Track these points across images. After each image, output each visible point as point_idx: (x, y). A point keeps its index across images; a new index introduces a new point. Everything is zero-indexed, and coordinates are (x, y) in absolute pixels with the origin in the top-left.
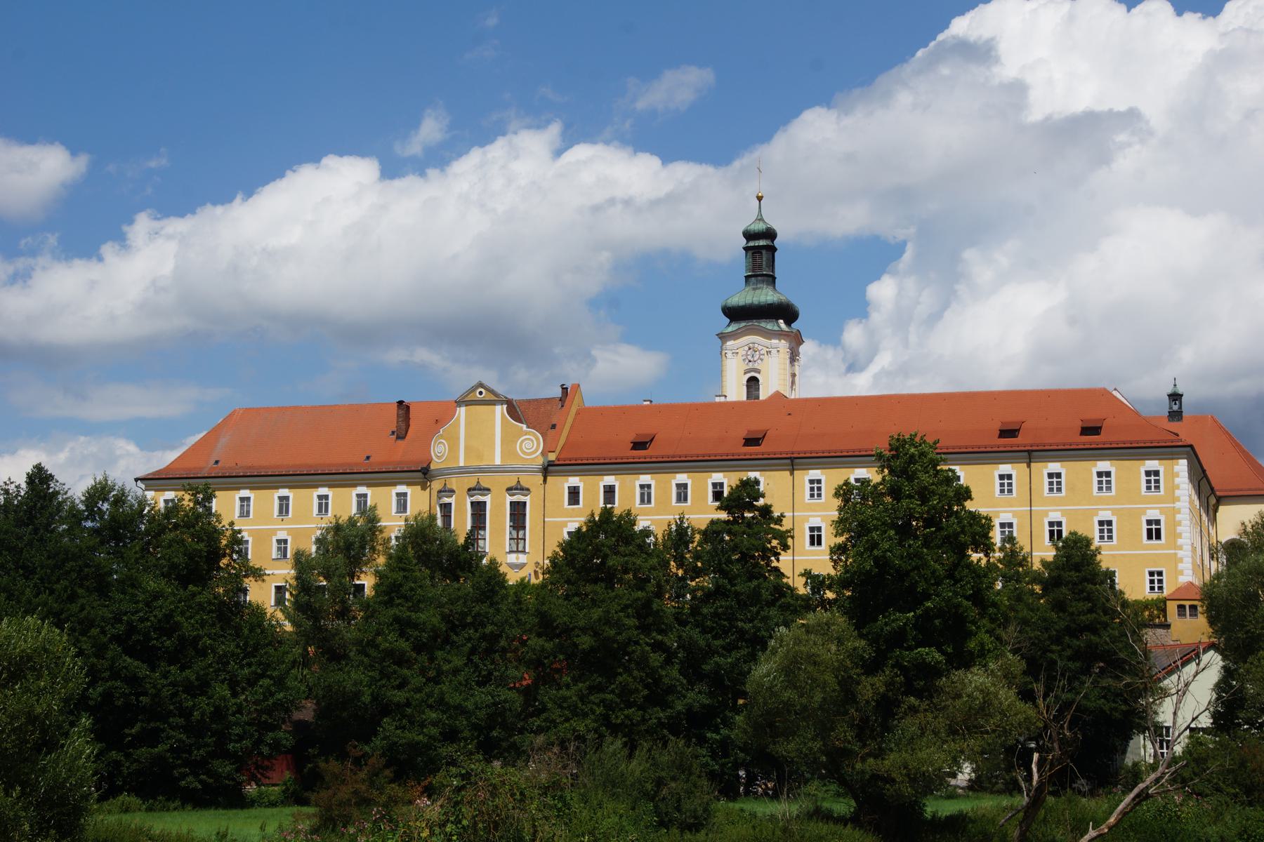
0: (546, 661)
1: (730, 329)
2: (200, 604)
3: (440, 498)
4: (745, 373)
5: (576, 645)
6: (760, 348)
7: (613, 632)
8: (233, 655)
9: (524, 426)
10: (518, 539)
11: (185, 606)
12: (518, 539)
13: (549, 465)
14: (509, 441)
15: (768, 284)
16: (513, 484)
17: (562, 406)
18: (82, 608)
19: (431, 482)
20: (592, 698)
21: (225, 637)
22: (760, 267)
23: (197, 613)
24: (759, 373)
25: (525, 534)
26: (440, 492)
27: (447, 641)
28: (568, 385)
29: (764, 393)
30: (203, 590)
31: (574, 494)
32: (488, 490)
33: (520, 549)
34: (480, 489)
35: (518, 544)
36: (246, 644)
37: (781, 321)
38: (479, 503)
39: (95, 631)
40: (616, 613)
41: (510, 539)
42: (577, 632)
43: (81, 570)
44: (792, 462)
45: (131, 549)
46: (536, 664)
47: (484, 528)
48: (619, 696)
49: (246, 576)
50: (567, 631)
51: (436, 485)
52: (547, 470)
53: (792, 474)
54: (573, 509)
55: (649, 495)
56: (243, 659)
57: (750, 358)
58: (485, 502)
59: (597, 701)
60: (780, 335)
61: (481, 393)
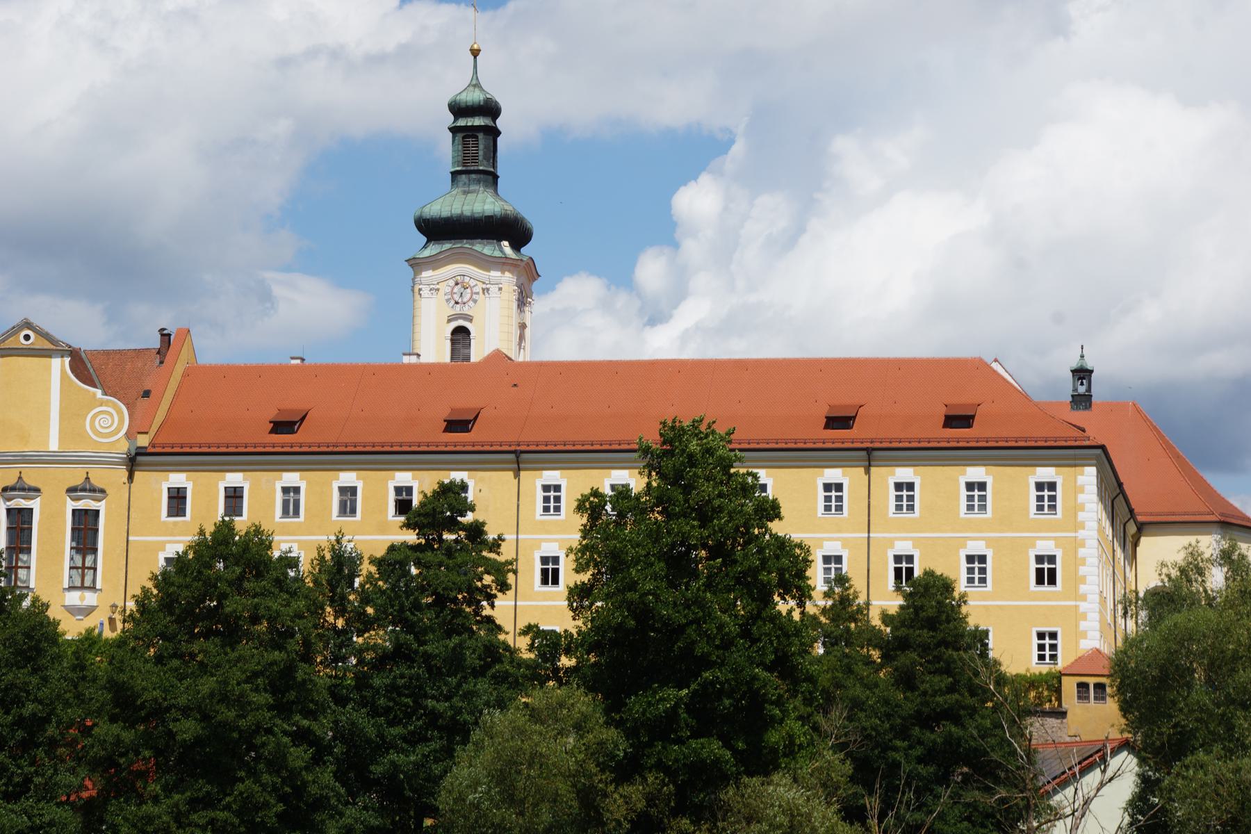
0: (122, 760)
1: (427, 253)
4: (449, 321)
5: (171, 735)
6: (472, 283)
7: (231, 714)
9: (99, 393)
10: (83, 567)
12: (83, 567)
13: (137, 454)
14: (72, 415)
15: (486, 186)
16: (78, 481)
17: (162, 362)
20: (194, 817)
22: (475, 158)
24: (471, 321)
25: (95, 561)
28: (171, 329)
29: (478, 351)
31: (177, 500)
32: (37, 490)
33: (88, 583)
34: (23, 489)
35: (84, 576)
37: (506, 243)
38: (20, 510)
40: (238, 684)
41: (71, 568)
42: (174, 713)
44: (518, 457)
46: (105, 764)
47: (28, 551)
48: (238, 814)
50: (158, 712)
52: (134, 461)
53: (517, 476)
54: (175, 523)
55: (297, 504)
57: (457, 297)
59: (202, 822)
60: (502, 264)
61: (27, 337)
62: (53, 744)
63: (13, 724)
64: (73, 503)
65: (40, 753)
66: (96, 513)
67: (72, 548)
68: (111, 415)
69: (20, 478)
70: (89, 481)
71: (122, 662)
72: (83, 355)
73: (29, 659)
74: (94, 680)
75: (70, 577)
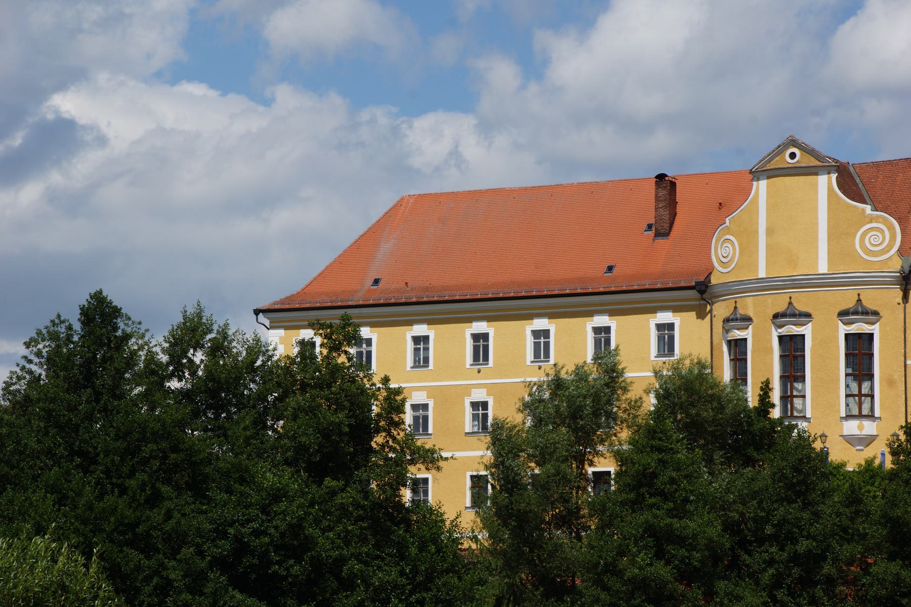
2: (342, 507)
3: (727, 331)
8: (396, 587)
9: (868, 208)
10: (860, 395)
11: (320, 509)
12: (860, 395)
16: (850, 304)
18: (168, 516)
19: (712, 304)
21: (383, 559)
23: (339, 521)
25: (872, 388)
26: (727, 320)
27: (735, 564)
30: (346, 485)
32: (808, 315)
33: (866, 411)
34: (794, 315)
36: (415, 570)
38: (792, 337)
39: (187, 552)
41: (847, 396)
43: (165, 457)
45: (238, 423)
47: (803, 379)
49: (413, 462)
51: (721, 310)
56: (412, 592)
58: (803, 336)
61: (793, 156)
62: (830, 582)
63: (789, 561)
64: (845, 327)
65: (819, 591)
66: (871, 336)
67: (847, 375)
68: (882, 231)
69: (790, 303)
70: (861, 304)
71: (895, 496)
72: (852, 169)
73: (799, 494)
74: (868, 514)
75: (847, 405)
